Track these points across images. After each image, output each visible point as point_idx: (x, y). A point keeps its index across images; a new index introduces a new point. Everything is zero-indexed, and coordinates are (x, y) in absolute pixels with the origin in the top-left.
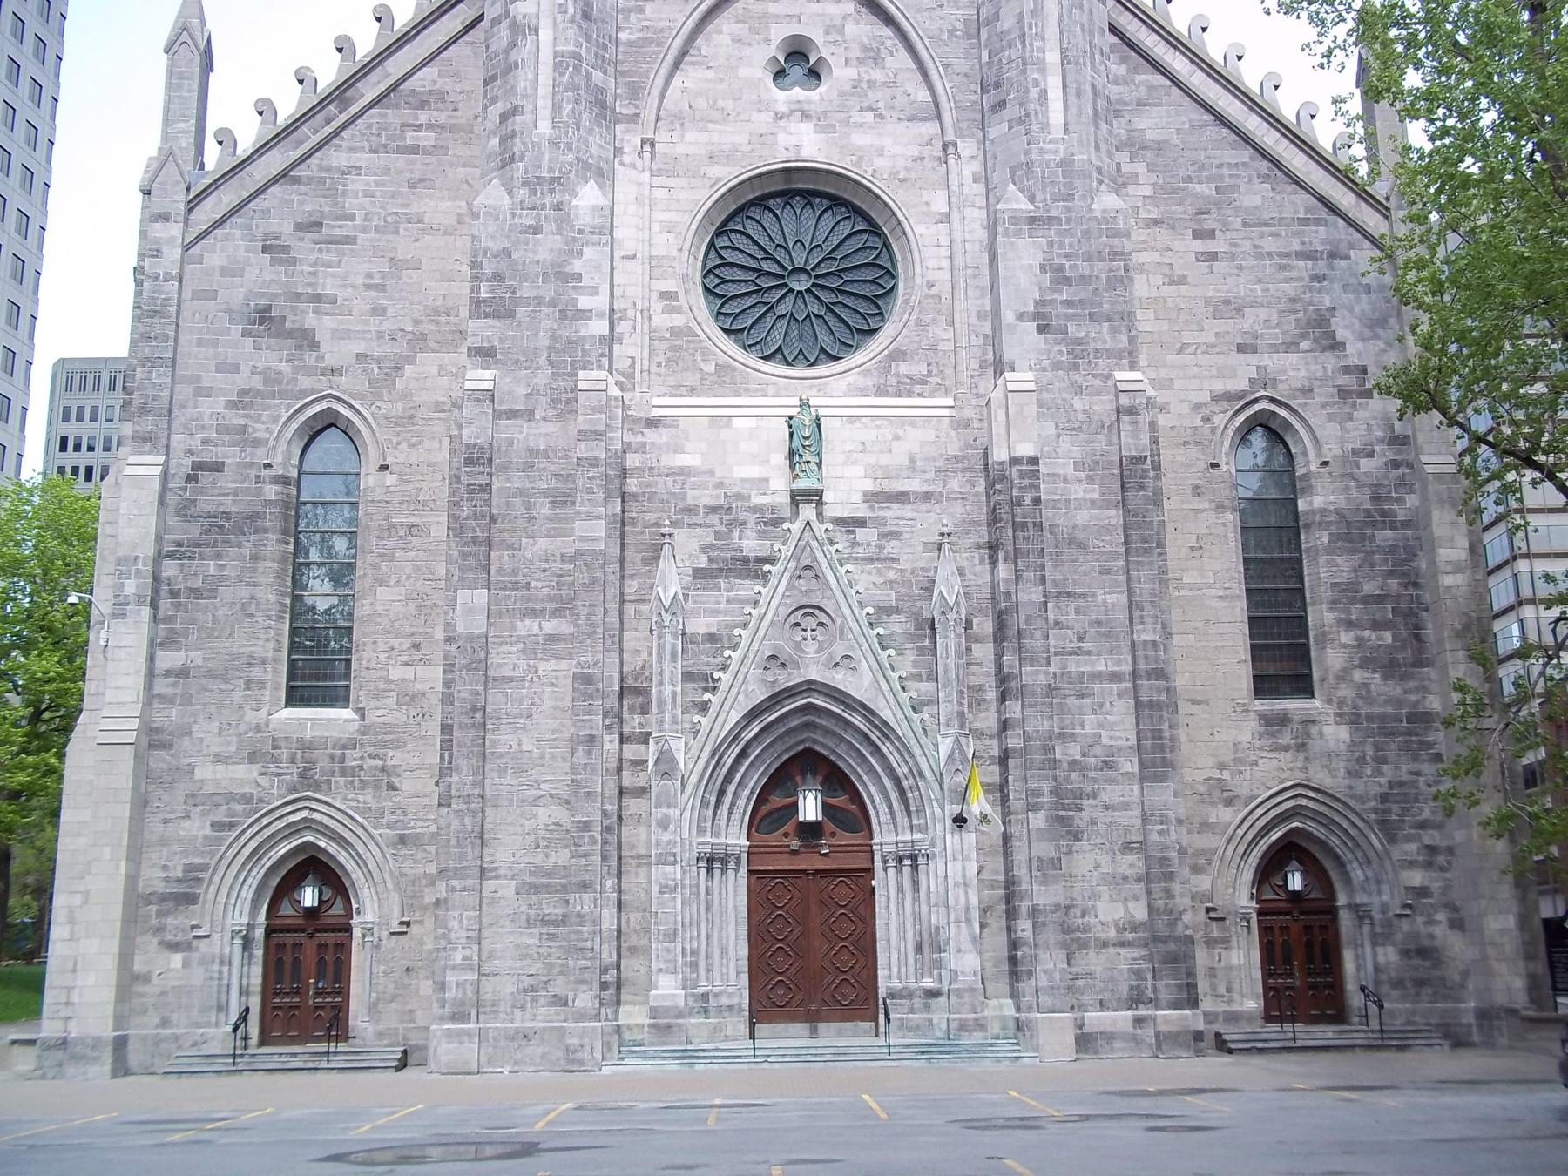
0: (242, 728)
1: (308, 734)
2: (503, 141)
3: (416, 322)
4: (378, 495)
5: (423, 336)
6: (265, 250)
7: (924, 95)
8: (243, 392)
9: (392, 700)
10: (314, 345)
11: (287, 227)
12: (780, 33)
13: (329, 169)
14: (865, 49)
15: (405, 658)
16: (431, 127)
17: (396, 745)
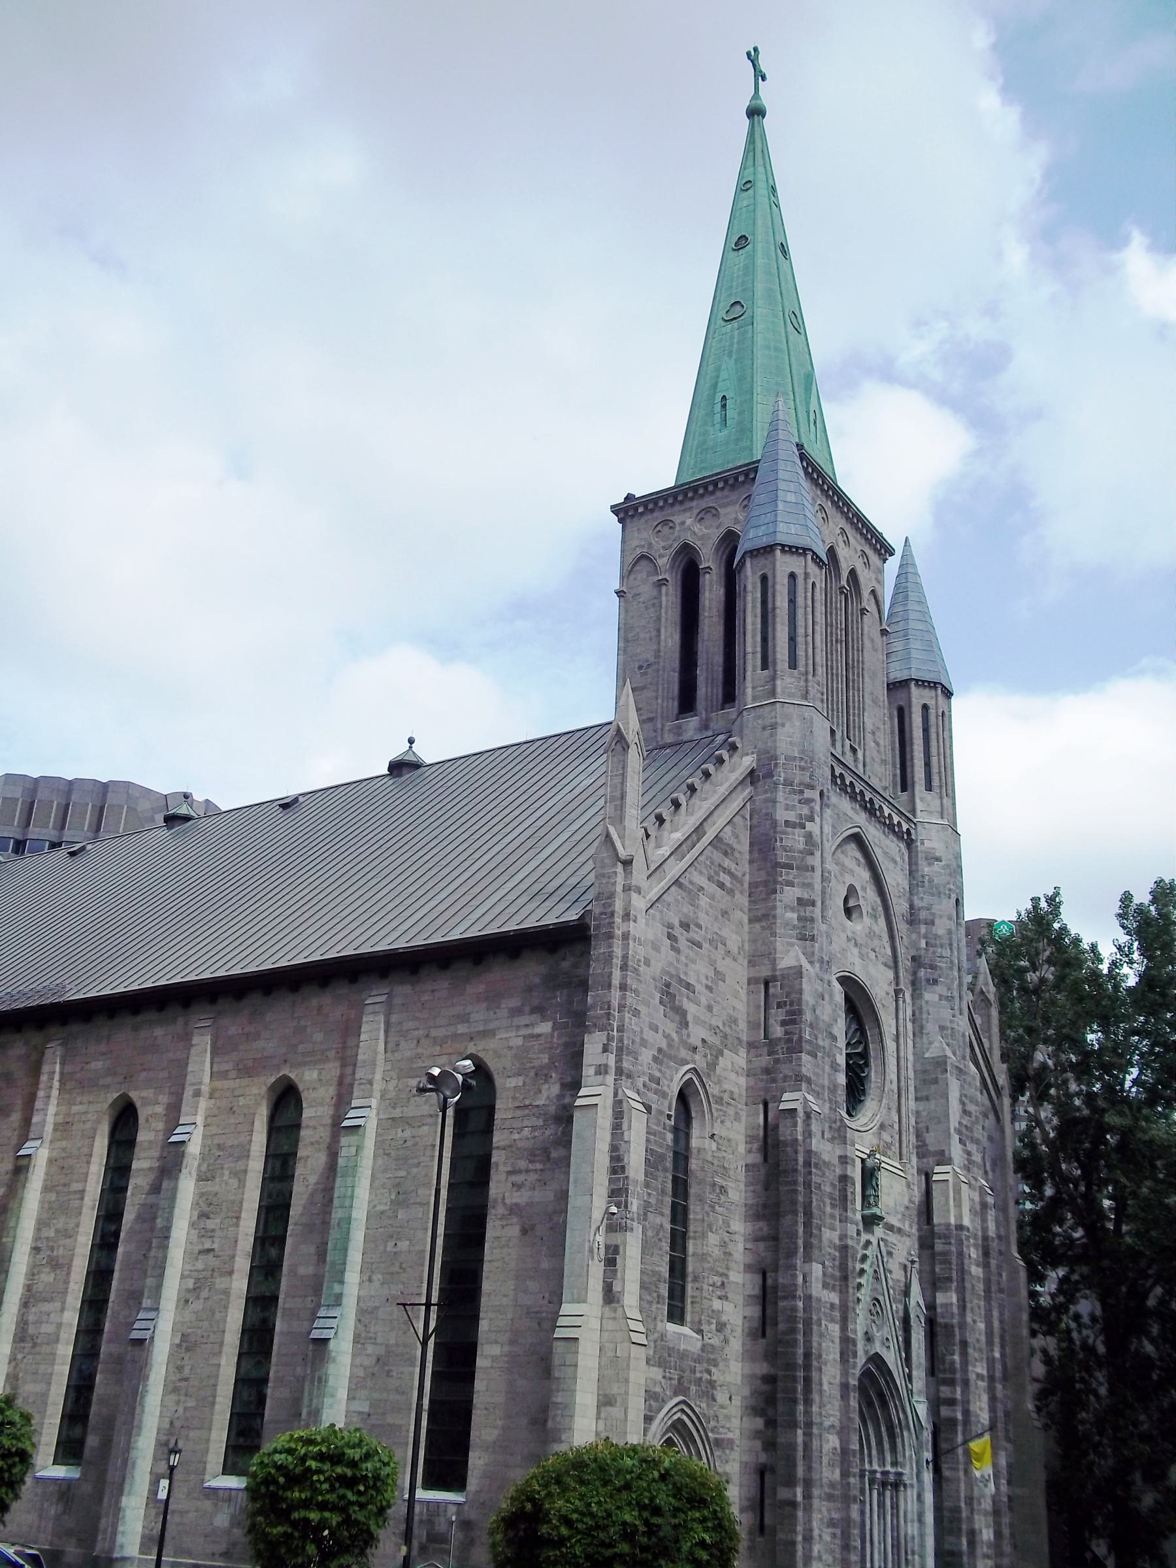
0: (656, 1335)
1: (682, 1347)
2: (800, 919)
3: (724, 1024)
5: (725, 1036)
7: (889, 951)
8: (660, 1050)
9: (713, 1326)
10: (687, 1024)
11: (677, 924)
12: (849, 880)
13: (691, 882)
14: (873, 909)
15: (719, 1293)
16: (730, 873)
17: (716, 1365)
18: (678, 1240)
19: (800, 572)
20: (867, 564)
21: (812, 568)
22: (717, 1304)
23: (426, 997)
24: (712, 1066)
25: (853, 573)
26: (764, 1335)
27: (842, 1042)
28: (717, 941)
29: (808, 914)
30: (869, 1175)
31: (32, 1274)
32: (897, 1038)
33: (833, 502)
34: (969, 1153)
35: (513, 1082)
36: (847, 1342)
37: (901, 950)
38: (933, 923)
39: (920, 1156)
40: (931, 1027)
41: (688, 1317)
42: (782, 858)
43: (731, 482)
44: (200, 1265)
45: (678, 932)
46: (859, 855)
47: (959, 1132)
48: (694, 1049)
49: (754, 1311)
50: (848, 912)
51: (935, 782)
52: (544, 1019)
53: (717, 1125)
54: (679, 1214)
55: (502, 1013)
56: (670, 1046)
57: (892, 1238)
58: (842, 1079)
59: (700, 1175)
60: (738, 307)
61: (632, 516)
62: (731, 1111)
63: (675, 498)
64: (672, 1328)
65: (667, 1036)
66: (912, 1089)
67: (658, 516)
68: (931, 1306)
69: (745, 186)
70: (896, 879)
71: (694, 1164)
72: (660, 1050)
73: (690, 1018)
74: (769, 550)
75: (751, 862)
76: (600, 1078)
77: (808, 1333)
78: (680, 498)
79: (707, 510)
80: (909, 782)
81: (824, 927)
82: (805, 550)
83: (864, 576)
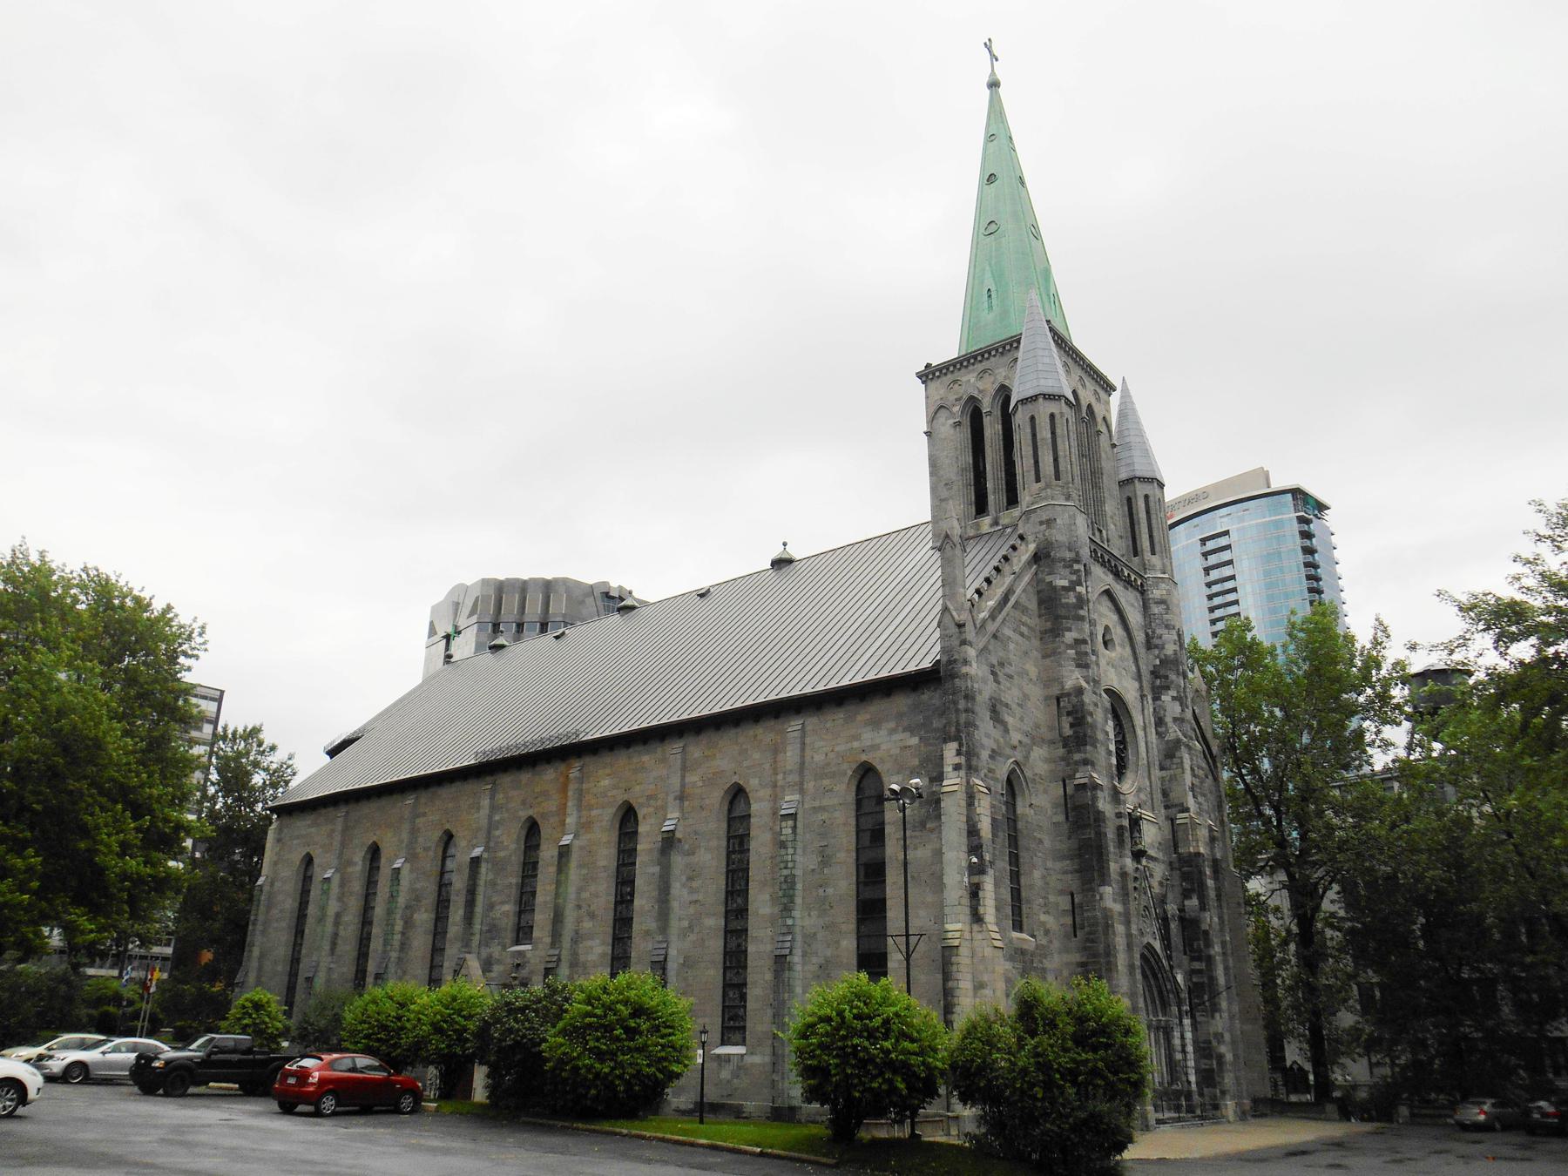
4: (1030, 820)
6: (993, 673)
8: (993, 751)
18: (1015, 876)
19: (1056, 412)
20: (1099, 399)
21: (1065, 409)
22: (1043, 918)
23: (828, 725)
24: (1027, 757)
25: (1090, 406)
26: (1075, 936)
27: (1112, 736)
28: (1023, 673)
29: (1083, 650)
30: (1135, 822)
31: (579, 921)
32: (1145, 729)
33: (1072, 358)
34: (1200, 804)
36: (1129, 935)
37: (1143, 668)
38: (1163, 648)
39: (1166, 807)
40: (1168, 720)
41: (1025, 927)
42: (1062, 612)
43: (1000, 350)
44: (692, 910)
45: (997, 669)
46: (1109, 604)
47: (1192, 789)
48: (1015, 748)
49: (1068, 920)
50: (1106, 644)
51: (1157, 548)
52: (913, 735)
53: (1033, 797)
54: (1014, 859)
55: (883, 732)
56: (999, 747)
57: (1151, 865)
58: (1114, 761)
59: (1025, 832)
60: (993, 225)
61: (932, 379)
62: (1041, 788)
63: (961, 364)
64: (1016, 935)
65: (997, 741)
66: (1157, 763)
67: (950, 377)
68: (1181, 910)
69: (991, 137)
70: (1135, 617)
71: (1020, 825)
72: (993, 751)
73: (1010, 727)
74: (1034, 398)
75: (1040, 616)
76: (957, 772)
77: (1106, 934)
78: (965, 364)
79: (984, 371)
80: (1139, 549)
81: (1094, 658)
82: (1059, 396)
83: (1098, 408)
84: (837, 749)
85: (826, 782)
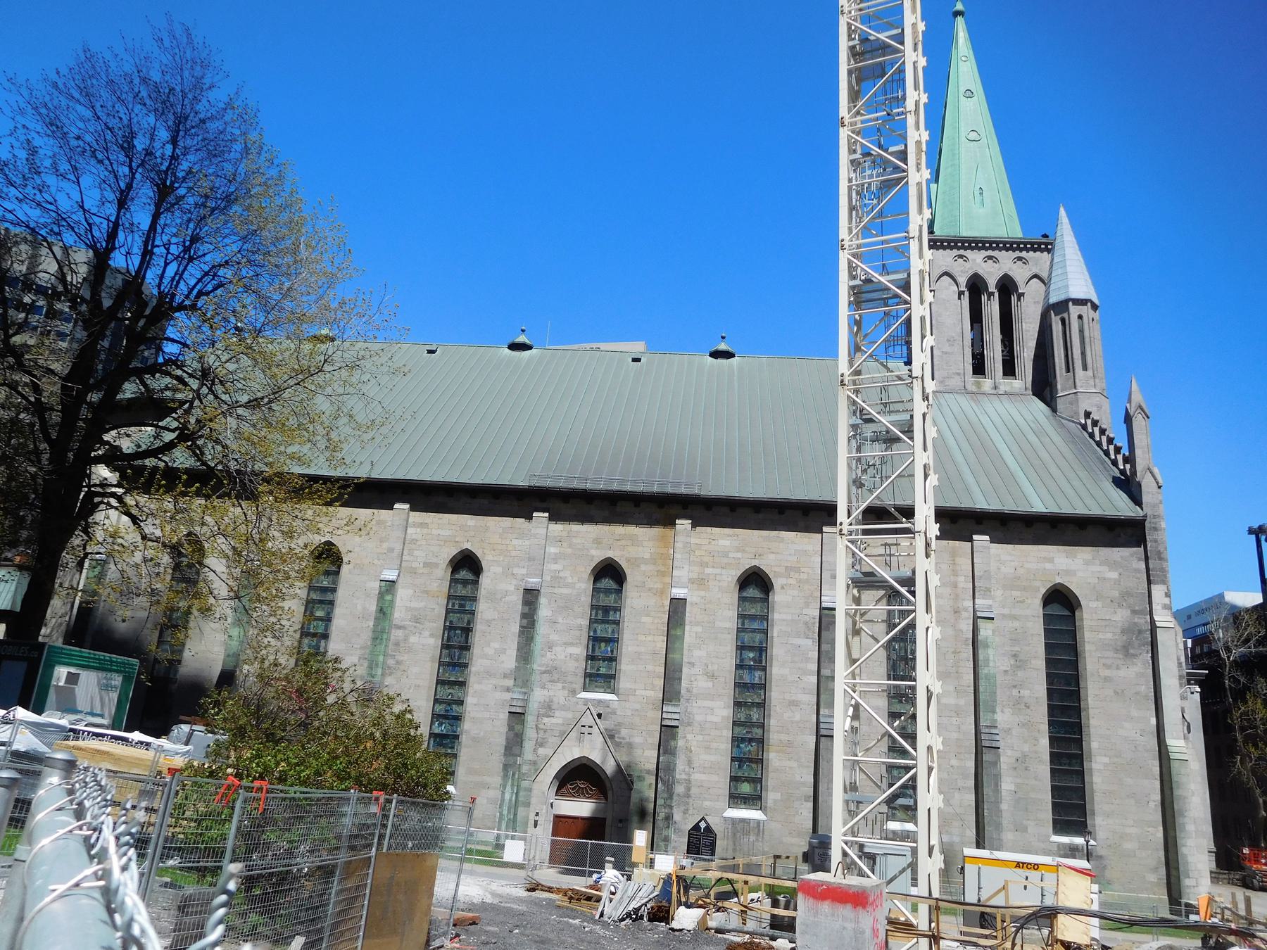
35: (1094, 604)
84: (1027, 565)
85: (1016, 593)
